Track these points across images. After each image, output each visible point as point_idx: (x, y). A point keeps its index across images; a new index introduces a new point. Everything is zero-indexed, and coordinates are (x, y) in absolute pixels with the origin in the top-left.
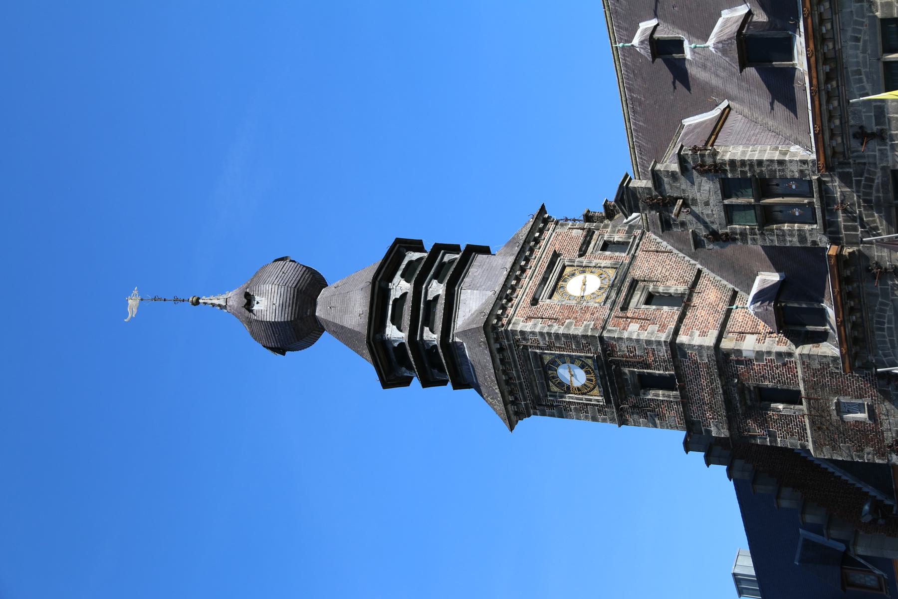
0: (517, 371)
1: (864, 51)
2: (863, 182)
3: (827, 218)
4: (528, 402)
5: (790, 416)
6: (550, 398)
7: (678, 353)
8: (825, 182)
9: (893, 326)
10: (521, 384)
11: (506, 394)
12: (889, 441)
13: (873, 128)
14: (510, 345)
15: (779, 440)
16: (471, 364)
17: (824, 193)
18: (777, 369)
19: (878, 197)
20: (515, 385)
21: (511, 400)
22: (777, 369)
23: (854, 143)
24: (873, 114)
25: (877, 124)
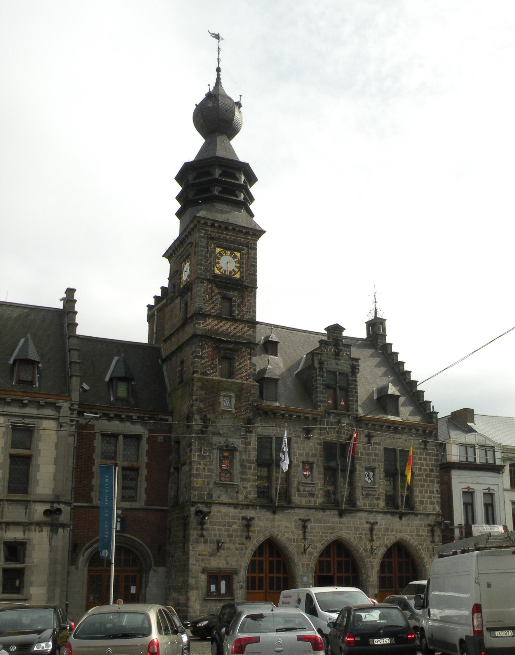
0: (231, 235)
1: (401, 443)
2: (349, 433)
3: (332, 414)
4: (209, 232)
5: (217, 370)
6: (213, 245)
7: (251, 325)
8: (349, 417)
9: (278, 431)
10: (223, 234)
11: (220, 224)
12: (209, 416)
13: (372, 441)
14: (248, 239)
15: (200, 360)
16: (232, 212)
17: (343, 415)
18: (246, 371)
19: (343, 437)
20: (223, 231)
21: (216, 224)
22: (246, 371)
23: (366, 431)
24: (378, 441)
25: (374, 442)
